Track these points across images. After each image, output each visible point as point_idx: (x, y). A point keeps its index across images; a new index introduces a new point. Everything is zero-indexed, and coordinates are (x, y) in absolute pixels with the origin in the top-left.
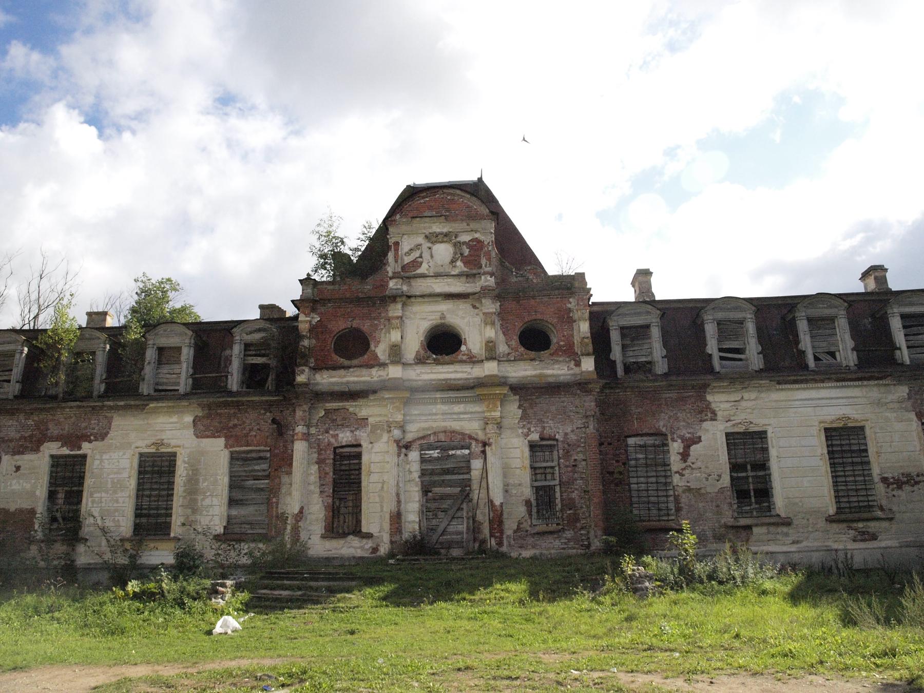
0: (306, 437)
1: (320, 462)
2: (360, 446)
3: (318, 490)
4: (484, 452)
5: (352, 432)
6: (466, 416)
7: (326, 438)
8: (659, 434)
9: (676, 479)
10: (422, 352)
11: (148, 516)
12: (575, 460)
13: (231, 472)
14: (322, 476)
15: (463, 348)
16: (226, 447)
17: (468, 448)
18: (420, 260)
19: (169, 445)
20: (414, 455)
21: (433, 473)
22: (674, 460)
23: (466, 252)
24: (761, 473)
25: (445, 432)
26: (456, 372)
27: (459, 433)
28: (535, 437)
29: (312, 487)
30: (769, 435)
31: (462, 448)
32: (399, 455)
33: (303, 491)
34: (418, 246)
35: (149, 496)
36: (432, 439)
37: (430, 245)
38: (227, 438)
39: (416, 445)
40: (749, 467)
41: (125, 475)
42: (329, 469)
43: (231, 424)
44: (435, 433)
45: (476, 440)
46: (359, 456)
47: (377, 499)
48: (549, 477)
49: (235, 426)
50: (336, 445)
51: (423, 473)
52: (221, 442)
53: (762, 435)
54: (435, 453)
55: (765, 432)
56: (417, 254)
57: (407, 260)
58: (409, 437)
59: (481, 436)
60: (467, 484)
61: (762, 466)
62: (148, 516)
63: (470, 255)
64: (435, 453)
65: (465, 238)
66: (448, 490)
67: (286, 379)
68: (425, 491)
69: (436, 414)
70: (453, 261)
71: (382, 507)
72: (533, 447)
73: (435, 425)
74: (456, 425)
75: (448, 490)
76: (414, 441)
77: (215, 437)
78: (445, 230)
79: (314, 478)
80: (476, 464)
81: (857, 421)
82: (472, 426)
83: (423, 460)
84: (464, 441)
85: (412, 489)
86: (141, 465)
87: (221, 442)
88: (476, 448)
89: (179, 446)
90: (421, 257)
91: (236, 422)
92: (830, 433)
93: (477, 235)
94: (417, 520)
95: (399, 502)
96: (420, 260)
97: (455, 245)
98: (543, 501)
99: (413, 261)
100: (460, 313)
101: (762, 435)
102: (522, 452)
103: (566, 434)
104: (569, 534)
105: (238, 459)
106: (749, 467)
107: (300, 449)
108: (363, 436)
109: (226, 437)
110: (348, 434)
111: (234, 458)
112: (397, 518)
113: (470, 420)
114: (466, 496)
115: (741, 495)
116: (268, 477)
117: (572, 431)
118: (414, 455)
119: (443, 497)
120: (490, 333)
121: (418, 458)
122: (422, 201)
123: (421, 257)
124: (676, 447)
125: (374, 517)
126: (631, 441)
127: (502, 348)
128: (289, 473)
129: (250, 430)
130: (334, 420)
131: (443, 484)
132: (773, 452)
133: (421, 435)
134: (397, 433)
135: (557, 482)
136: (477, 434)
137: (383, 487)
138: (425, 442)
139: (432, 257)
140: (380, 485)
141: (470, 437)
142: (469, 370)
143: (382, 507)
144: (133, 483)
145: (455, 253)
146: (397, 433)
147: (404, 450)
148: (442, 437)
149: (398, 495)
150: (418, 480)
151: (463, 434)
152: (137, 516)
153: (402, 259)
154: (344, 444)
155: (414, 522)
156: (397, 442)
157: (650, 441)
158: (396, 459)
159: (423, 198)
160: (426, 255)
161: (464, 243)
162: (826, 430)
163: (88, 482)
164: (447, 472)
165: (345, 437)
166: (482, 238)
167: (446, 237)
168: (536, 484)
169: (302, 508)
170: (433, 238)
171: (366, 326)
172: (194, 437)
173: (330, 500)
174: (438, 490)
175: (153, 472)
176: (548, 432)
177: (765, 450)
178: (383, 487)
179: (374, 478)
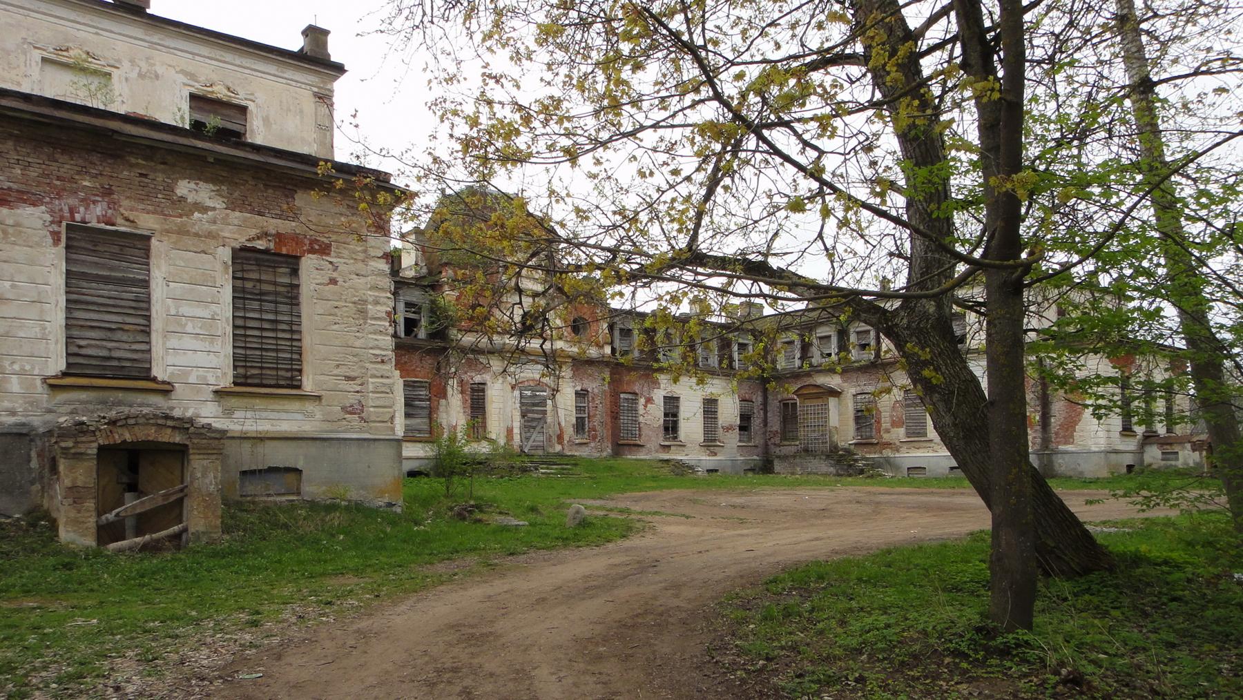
8: (636, 394)
9: (641, 419)
14: (465, 402)
22: (641, 408)
33: (454, 413)
46: (483, 391)
53: (678, 399)
54: (529, 393)
60: (545, 412)
61: (675, 415)
64: (529, 393)
66: (536, 416)
67: (439, 334)
68: (523, 416)
72: (577, 393)
75: (536, 416)
98: (580, 426)
101: (678, 399)
104: (592, 445)
108: (487, 377)
111: (406, 385)
112: (510, 431)
114: (543, 420)
115: (666, 429)
116: (429, 400)
118: (517, 393)
119: (533, 420)
124: (642, 401)
125: (495, 427)
130: (473, 365)
131: (533, 412)
132: (682, 409)
157: (630, 396)
164: (534, 405)
165: (478, 379)
174: (530, 415)
177: (678, 407)
179: (495, 405)
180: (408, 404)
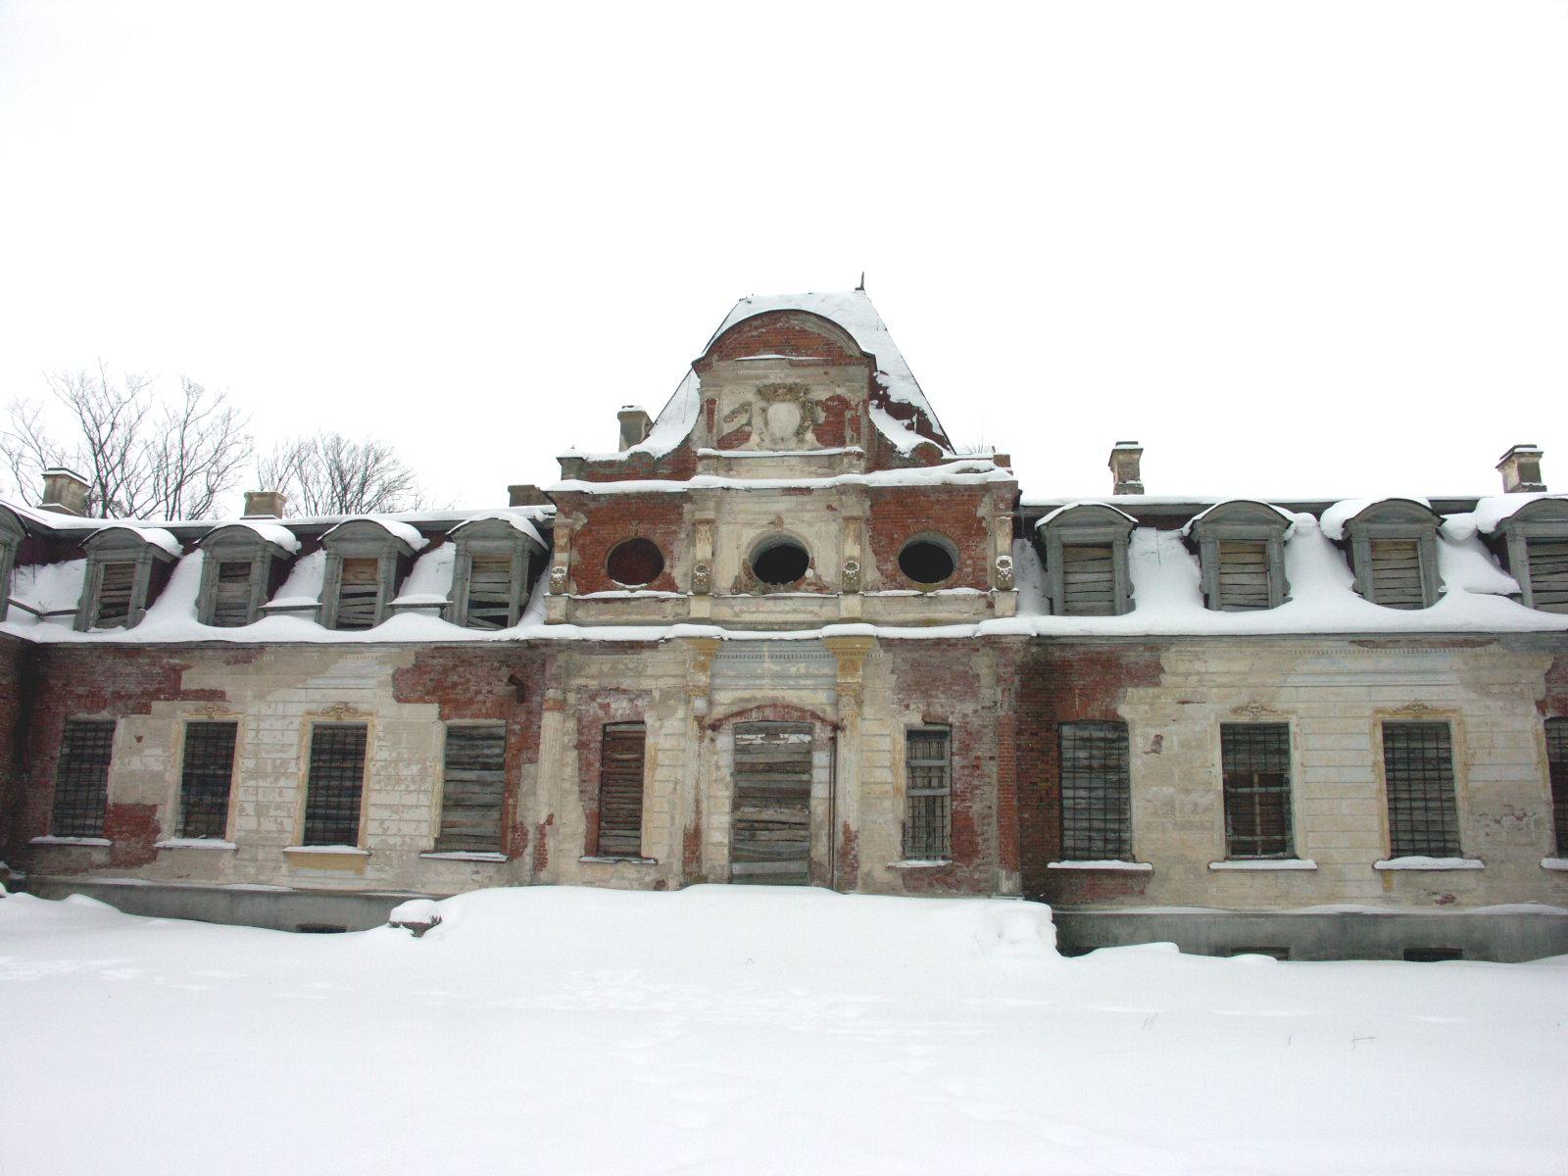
0: (560, 706)
1: (581, 746)
2: (643, 722)
3: (576, 789)
4: (834, 740)
5: (631, 700)
6: (808, 682)
7: (593, 709)
10: (744, 578)
11: (326, 818)
12: (978, 758)
13: (447, 756)
14: (584, 765)
15: (809, 573)
16: (442, 717)
17: (810, 731)
18: (747, 429)
19: (356, 711)
20: (725, 741)
21: (753, 769)
23: (822, 416)
24: (1274, 790)
25: (775, 706)
26: (795, 611)
27: (796, 708)
28: (916, 720)
29: (567, 785)
30: (1292, 728)
31: (798, 731)
32: (701, 739)
34: (745, 407)
35: (328, 788)
36: (755, 716)
37: (763, 404)
38: (442, 703)
39: (728, 727)
40: (1256, 779)
41: (292, 753)
42: (595, 757)
43: (448, 683)
44: (758, 708)
45: (823, 721)
47: (666, 807)
48: (935, 782)
49: (455, 685)
50: (606, 721)
51: (740, 769)
52: (432, 710)
53: (1280, 731)
54: (757, 739)
55: (1286, 726)
56: (743, 419)
57: (728, 428)
58: (719, 712)
59: (830, 714)
61: (1279, 778)
62: (326, 818)
63: (827, 423)
65: (821, 394)
69: (761, 677)
70: (799, 433)
71: (673, 818)
72: (912, 735)
73: (759, 694)
74: (791, 696)
76: (727, 717)
77: (425, 702)
78: (790, 381)
79: (570, 770)
80: (820, 759)
81: (1435, 711)
82: (816, 698)
83: (740, 749)
84: (803, 719)
85: (719, 793)
87: (432, 710)
88: (822, 733)
89: (371, 714)
90: (749, 424)
91: (455, 678)
92: (1392, 733)
93: (839, 391)
94: (726, 841)
95: (698, 812)
96: (747, 429)
97: (803, 406)
99: (737, 431)
100: (807, 516)
101: (1280, 731)
102: (894, 741)
103: (965, 716)
105: (458, 737)
106: (1256, 779)
109: (440, 703)
110: (625, 704)
111: (452, 734)
113: (815, 689)
117: (976, 711)
118: (725, 741)
120: (852, 549)
121: (731, 746)
122: (754, 333)
123: (749, 424)
126: (1067, 731)
127: (871, 575)
128: (533, 761)
129: (478, 692)
132: (1296, 757)
133: (736, 709)
134: (700, 704)
135: (947, 791)
136: (824, 711)
137: (675, 789)
138: (741, 720)
139: (766, 423)
140: (672, 786)
141: (814, 716)
142: (816, 609)
143: (673, 818)
144: (304, 767)
145: (804, 419)
146: (700, 704)
147: (709, 733)
148: (769, 713)
149: (697, 802)
150: (729, 779)
151: (802, 710)
152: (309, 817)
153: (720, 430)
154: (618, 719)
155: (720, 844)
156: (699, 719)
158: (695, 745)
159: (756, 328)
160: (757, 421)
161: (818, 403)
162: (1386, 726)
165: (620, 708)
166: (848, 396)
167: (792, 392)
168: (916, 793)
169: (551, 816)
170: (769, 393)
171: (657, 538)
172: (394, 701)
173: (595, 805)
175: (332, 752)
176: (938, 710)
178: (675, 789)
179: (661, 774)
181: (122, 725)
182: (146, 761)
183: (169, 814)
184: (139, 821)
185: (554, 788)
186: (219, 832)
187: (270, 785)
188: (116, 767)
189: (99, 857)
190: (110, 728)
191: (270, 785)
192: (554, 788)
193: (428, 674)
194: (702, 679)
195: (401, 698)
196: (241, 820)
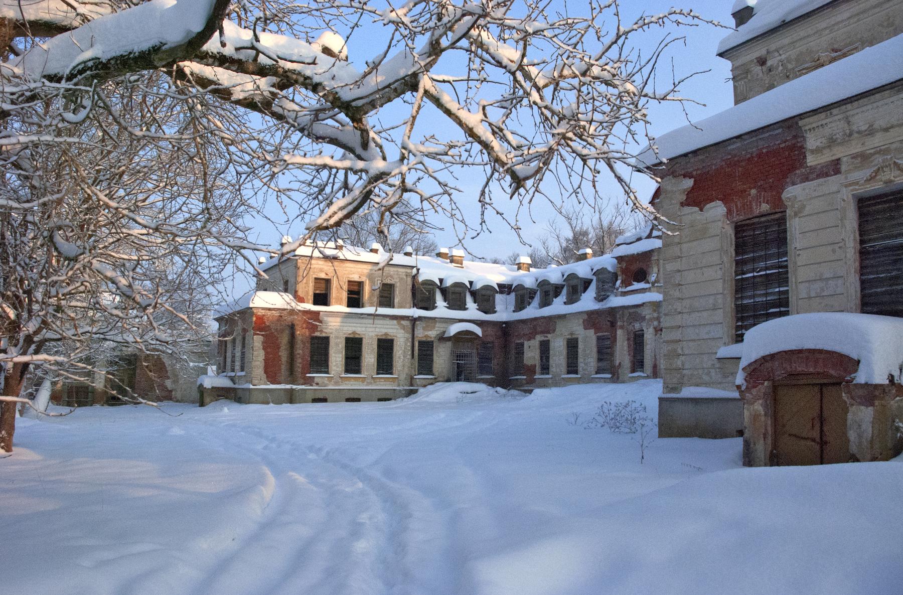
0: (622, 327)
1: (628, 339)
7: (631, 327)
46: (643, 335)
52: (592, 331)
79: (626, 348)
86: (568, 344)
87: (592, 331)
95: (656, 359)
107: (619, 332)
108: (644, 324)
111: (599, 338)
134: (656, 323)
144: (565, 352)
156: (655, 328)
163: (551, 352)
165: (637, 326)
180: (599, 352)
181: (526, 343)
182: (531, 355)
183: (538, 369)
184: (531, 370)
185: (622, 353)
186: (548, 374)
187: (558, 358)
188: (525, 355)
189: (524, 382)
190: (522, 345)
191: (558, 358)
192: (622, 353)
193: (592, 319)
194: (655, 315)
195: (585, 329)
196: (553, 369)
